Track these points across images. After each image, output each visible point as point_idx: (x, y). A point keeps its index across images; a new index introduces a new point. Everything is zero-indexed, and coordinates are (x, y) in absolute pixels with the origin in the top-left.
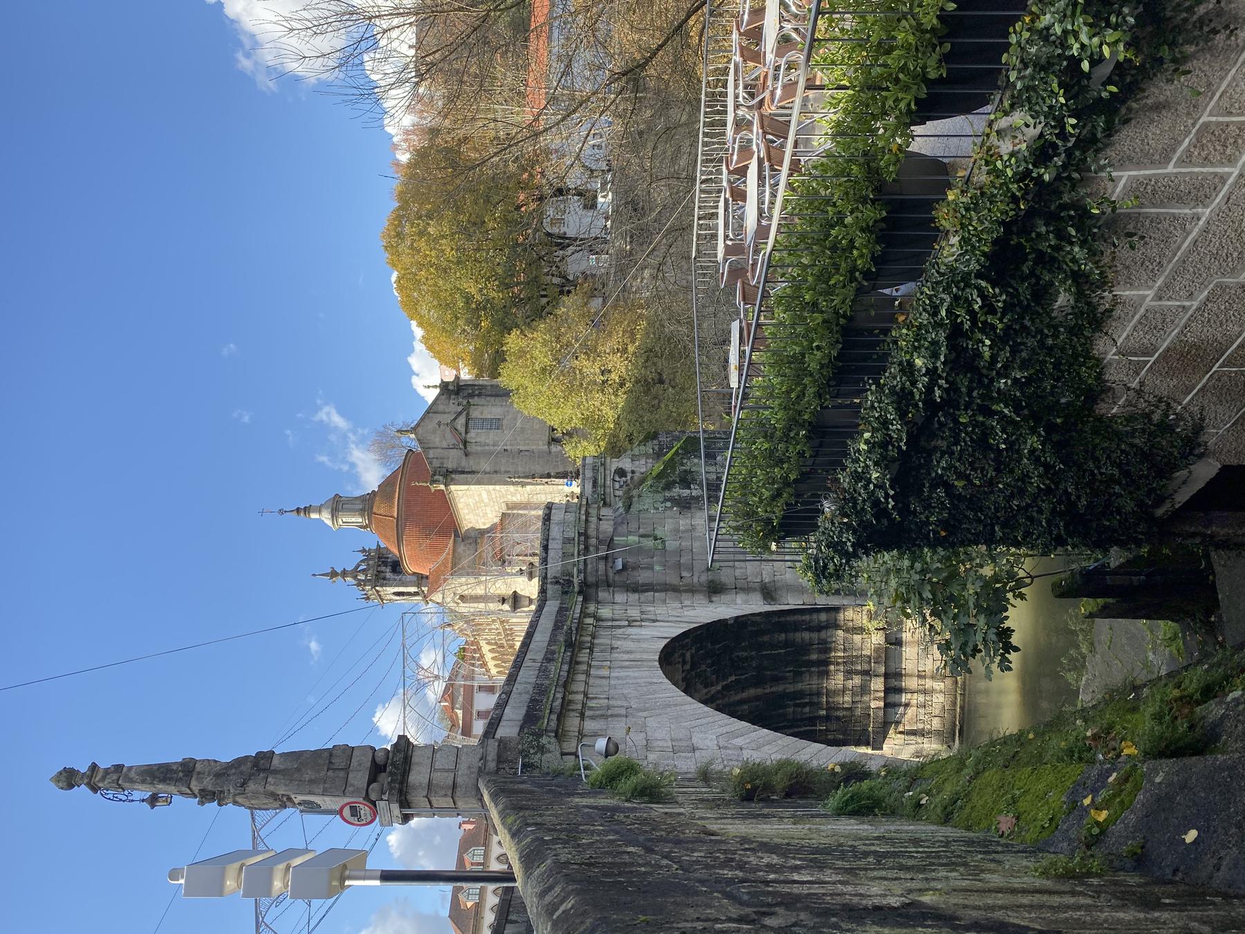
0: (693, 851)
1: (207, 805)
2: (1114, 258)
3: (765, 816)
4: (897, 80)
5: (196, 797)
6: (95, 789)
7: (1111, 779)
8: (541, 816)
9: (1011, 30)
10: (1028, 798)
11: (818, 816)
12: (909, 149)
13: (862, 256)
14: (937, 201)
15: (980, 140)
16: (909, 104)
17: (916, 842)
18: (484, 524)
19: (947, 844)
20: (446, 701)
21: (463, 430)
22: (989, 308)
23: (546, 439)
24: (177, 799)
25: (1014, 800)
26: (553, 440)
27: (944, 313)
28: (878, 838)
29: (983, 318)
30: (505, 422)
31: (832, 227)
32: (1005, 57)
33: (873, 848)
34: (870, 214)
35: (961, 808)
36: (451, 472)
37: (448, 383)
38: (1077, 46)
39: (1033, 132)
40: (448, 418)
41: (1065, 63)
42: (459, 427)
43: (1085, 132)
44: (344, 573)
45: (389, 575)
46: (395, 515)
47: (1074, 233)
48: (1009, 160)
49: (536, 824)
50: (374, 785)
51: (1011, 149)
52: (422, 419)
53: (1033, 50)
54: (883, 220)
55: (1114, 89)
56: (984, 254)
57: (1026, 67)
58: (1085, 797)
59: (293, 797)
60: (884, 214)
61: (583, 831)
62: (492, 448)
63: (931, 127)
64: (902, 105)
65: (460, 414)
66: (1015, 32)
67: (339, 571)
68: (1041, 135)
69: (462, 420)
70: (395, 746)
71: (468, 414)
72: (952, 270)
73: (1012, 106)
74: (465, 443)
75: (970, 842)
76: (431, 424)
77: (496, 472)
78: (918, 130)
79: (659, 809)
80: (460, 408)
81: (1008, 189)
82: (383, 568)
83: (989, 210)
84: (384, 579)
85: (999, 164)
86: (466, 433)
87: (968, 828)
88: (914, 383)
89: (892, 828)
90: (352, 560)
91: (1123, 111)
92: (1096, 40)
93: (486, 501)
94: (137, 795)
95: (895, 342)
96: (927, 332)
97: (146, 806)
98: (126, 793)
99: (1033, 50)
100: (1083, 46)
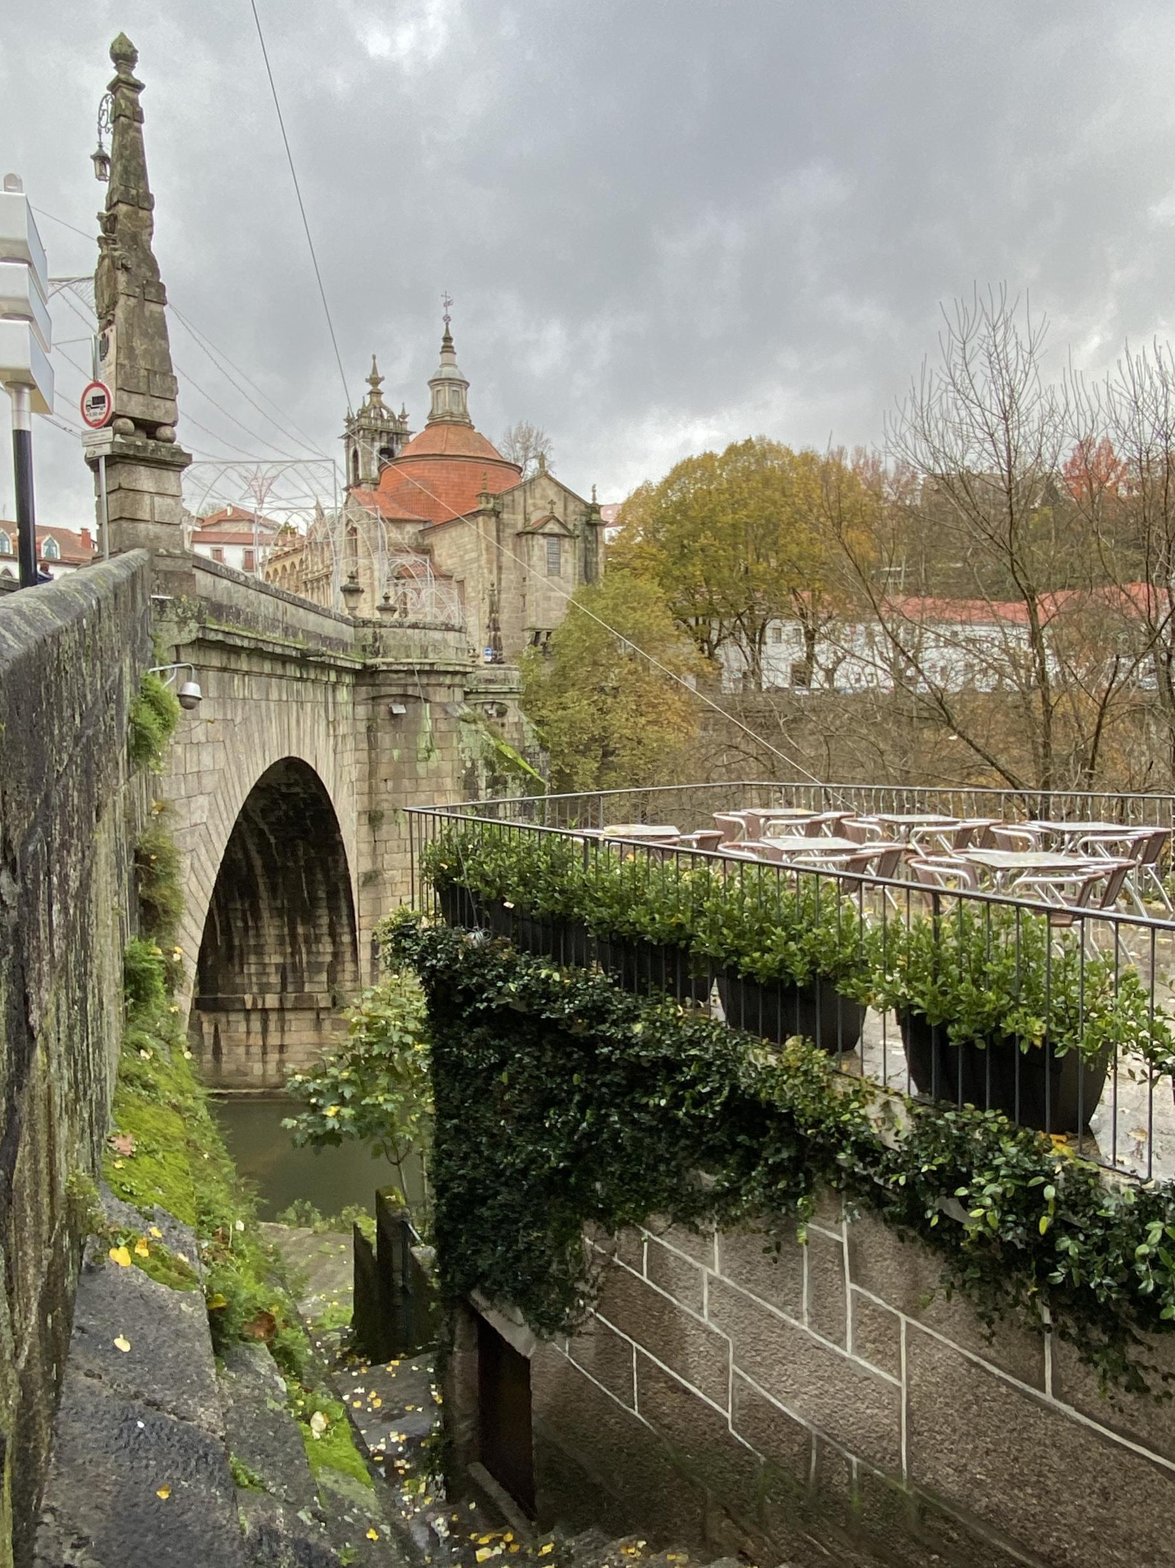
0: (80, 791)
1: (98, 223)
2: (753, 1232)
3: (120, 877)
4: (945, 993)
5: (108, 209)
6: (114, 87)
7: (181, 1256)
8: (109, 617)
9: (999, 1111)
10: (155, 1168)
11: (122, 936)
12: (869, 1008)
13: (754, 961)
14: (814, 1040)
15: (880, 1083)
16: (919, 1007)
17: (99, 1045)
19: (100, 1080)
21: (546, 530)
22: (700, 1101)
23: (539, 626)
24: (105, 187)
25: (151, 1153)
26: (538, 634)
27: (693, 1052)
28: (101, 1002)
29: (687, 1095)
30: (556, 578)
31: (785, 929)
32: (970, 1106)
33: (90, 997)
34: (799, 968)
35: (139, 1095)
37: (598, 512)
38: (982, 1181)
39: (890, 1140)
40: (559, 512)
41: (964, 1170)
43: (889, 1194)
44: (375, 393)
45: (378, 445)
47: (780, 1186)
48: (860, 1116)
49: (99, 610)
50: (131, 424)
51: (872, 1117)
52: (558, 484)
53: (977, 1135)
54: (793, 983)
55: (934, 1222)
56: (757, 1093)
57: (958, 1129)
58: (159, 1228)
59: (113, 327)
60: (799, 984)
61: (94, 665)
63: (895, 1029)
64: (917, 1000)
66: (997, 1116)
68: (887, 1149)
70: (179, 452)
72: (740, 1059)
73: (918, 1116)
75: (101, 1105)
76: (552, 493)
78: (892, 1015)
79: (122, 754)
80: (571, 527)
81: (828, 1116)
82: (385, 438)
83: (805, 1096)
84: (373, 440)
85: (855, 1105)
87: (115, 1103)
88: (614, 1023)
89: (112, 1018)
90: (393, 403)
91: (912, 1233)
92: (988, 1201)
94: (108, 140)
95: (659, 1002)
96: (671, 1035)
97: (94, 149)
98: (110, 125)
99: (977, 1135)
100: (982, 1188)
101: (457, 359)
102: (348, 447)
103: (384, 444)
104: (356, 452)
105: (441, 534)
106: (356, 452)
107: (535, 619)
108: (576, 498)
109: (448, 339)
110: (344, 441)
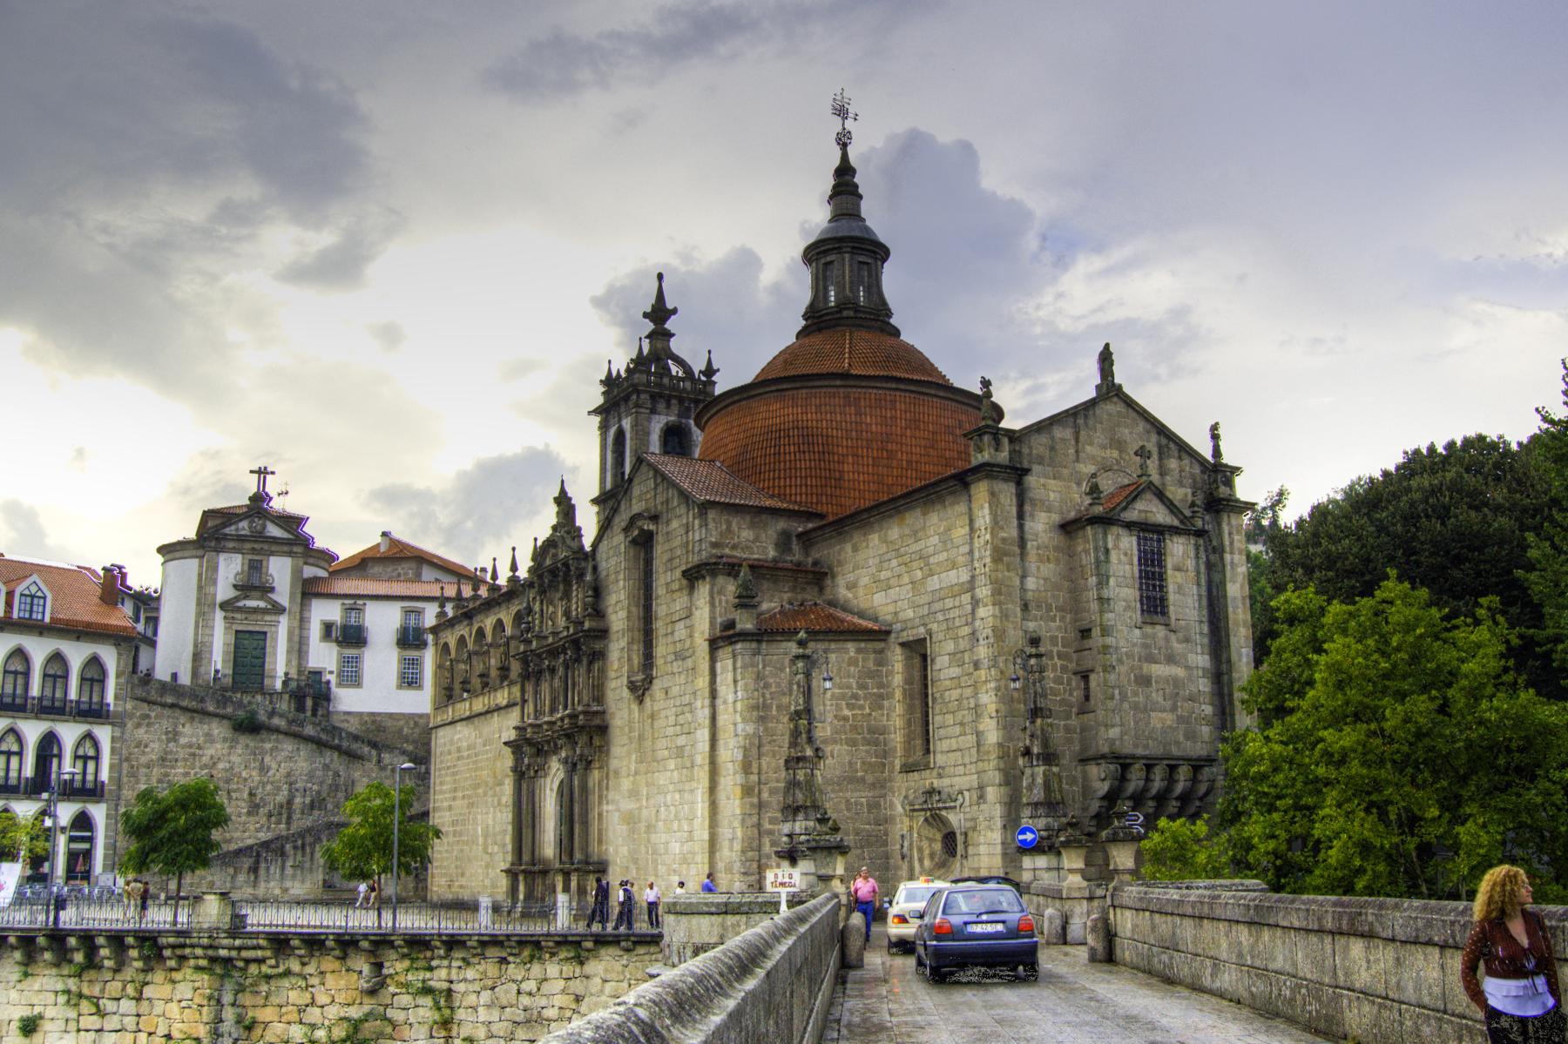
18: (852, 586)
20: (390, 548)
21: (1132, 515)
23: (1128, 749)
26: (1125, 767)
30: (1160, 631)
36: (1019, 483)
37: (1229, 483)
42: (1140, 505)
44: (660, 335)
46: (853, 372)
62: (1093, 594)
65: (1171, 506)
67: (669, 325)
69: (1160, 515)
71: (1175, 531)
74: (1105, 521)
76: (1134, 435)
77: (1025, 607)
82: (675, 409)
86: (1129, 526)
93: (934, 583)
101: (867, 209)
102: (604, 427)
103: (672, 418)
104: (620, 435)
105: (857, 537)
106: (620, 435)
107: (1114, 734)
108: (1184, 449)
109: (845, 172)
110: (597, 420)
